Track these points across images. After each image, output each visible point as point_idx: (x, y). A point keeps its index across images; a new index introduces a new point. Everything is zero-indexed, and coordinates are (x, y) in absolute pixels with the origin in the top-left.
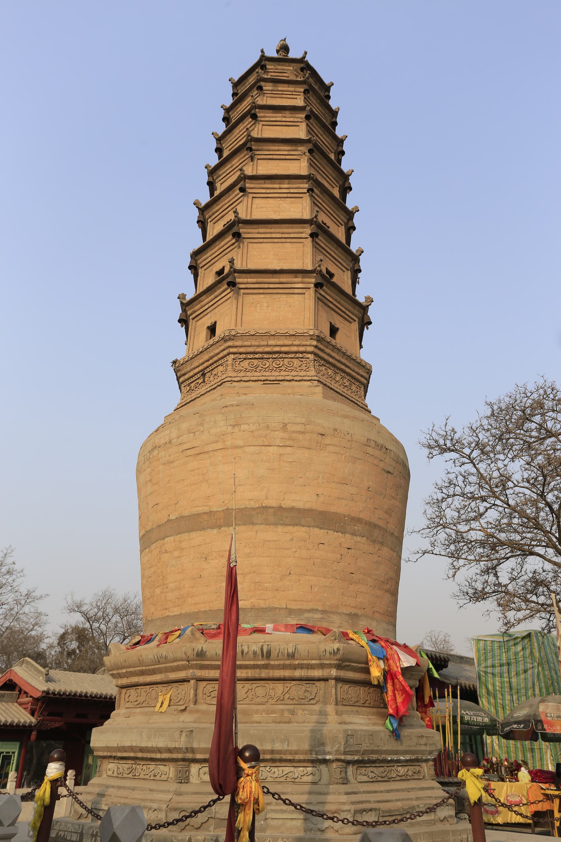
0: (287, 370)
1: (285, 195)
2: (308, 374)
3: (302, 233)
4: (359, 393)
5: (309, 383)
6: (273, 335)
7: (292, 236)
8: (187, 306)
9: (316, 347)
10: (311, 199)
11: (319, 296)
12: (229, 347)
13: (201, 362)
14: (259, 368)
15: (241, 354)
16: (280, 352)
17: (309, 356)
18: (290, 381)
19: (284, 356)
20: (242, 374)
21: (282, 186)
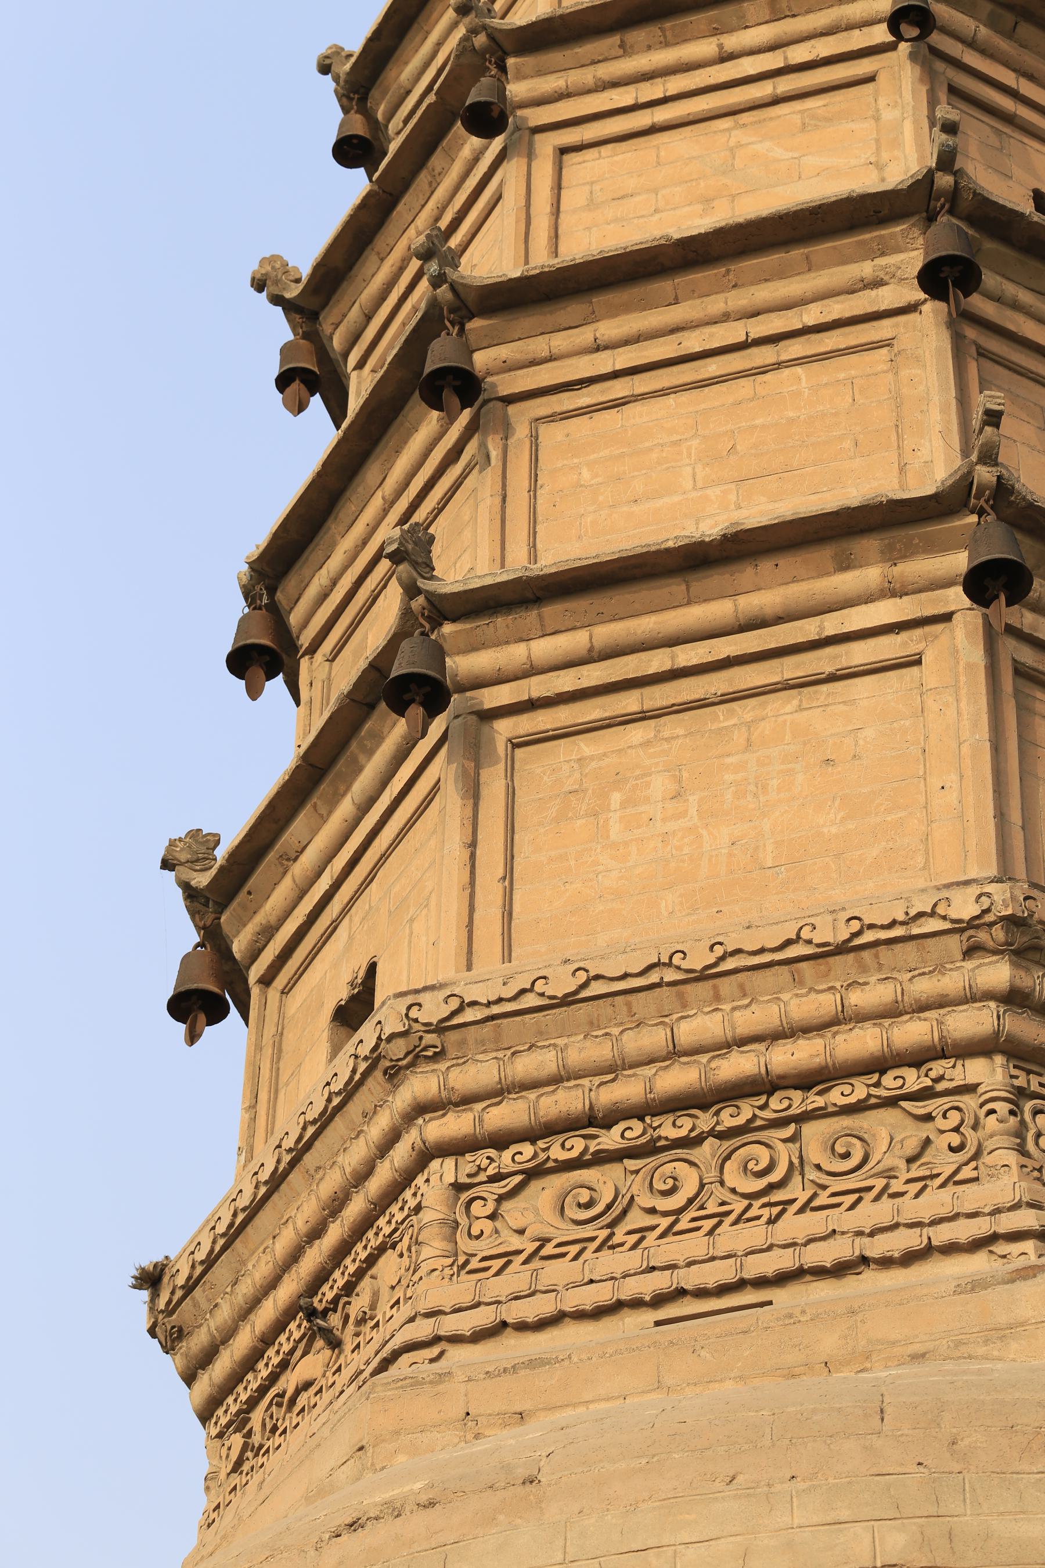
0: (823, 1199)
2: (971, 1197)
3: (877, 283)
5: (978, 1263)
6: (703, 976)
7: (812, 315)
8: (222, 907)
9: (1013, 998)
10: (930, 76)
11: (1028, 656)
12: (422, 1109)
13: (282, 1246)
14: (636, 1219)
15: (501, 1141)
17: (975, 1070)
18: (840, 1270)
19: (798, 1101)
20: (517, 1277)
21: (733, 41)
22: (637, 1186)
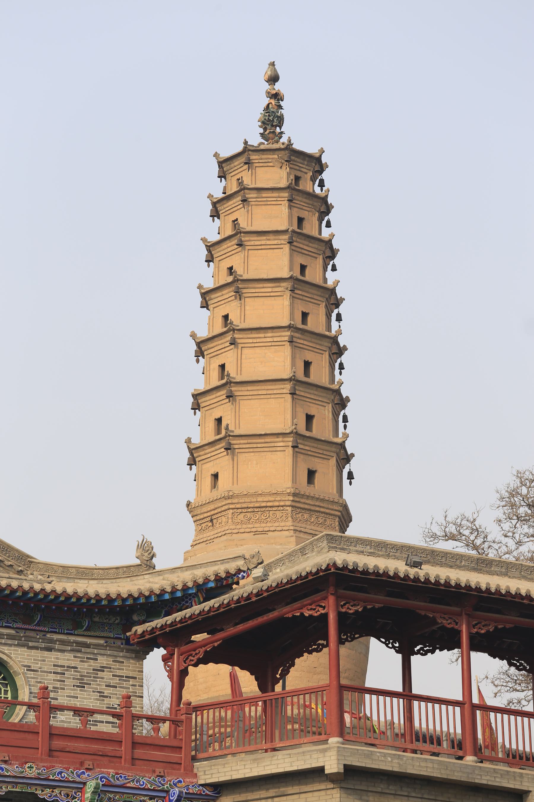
1: (270, 344)
4: (333, 525)
9: (293, 501)
13: (209, 509)
14: (252, 520)
15: (238, 509)
16: (266, 507)
17: (288, 508)
19: (270, 509)
22: (252, 516)
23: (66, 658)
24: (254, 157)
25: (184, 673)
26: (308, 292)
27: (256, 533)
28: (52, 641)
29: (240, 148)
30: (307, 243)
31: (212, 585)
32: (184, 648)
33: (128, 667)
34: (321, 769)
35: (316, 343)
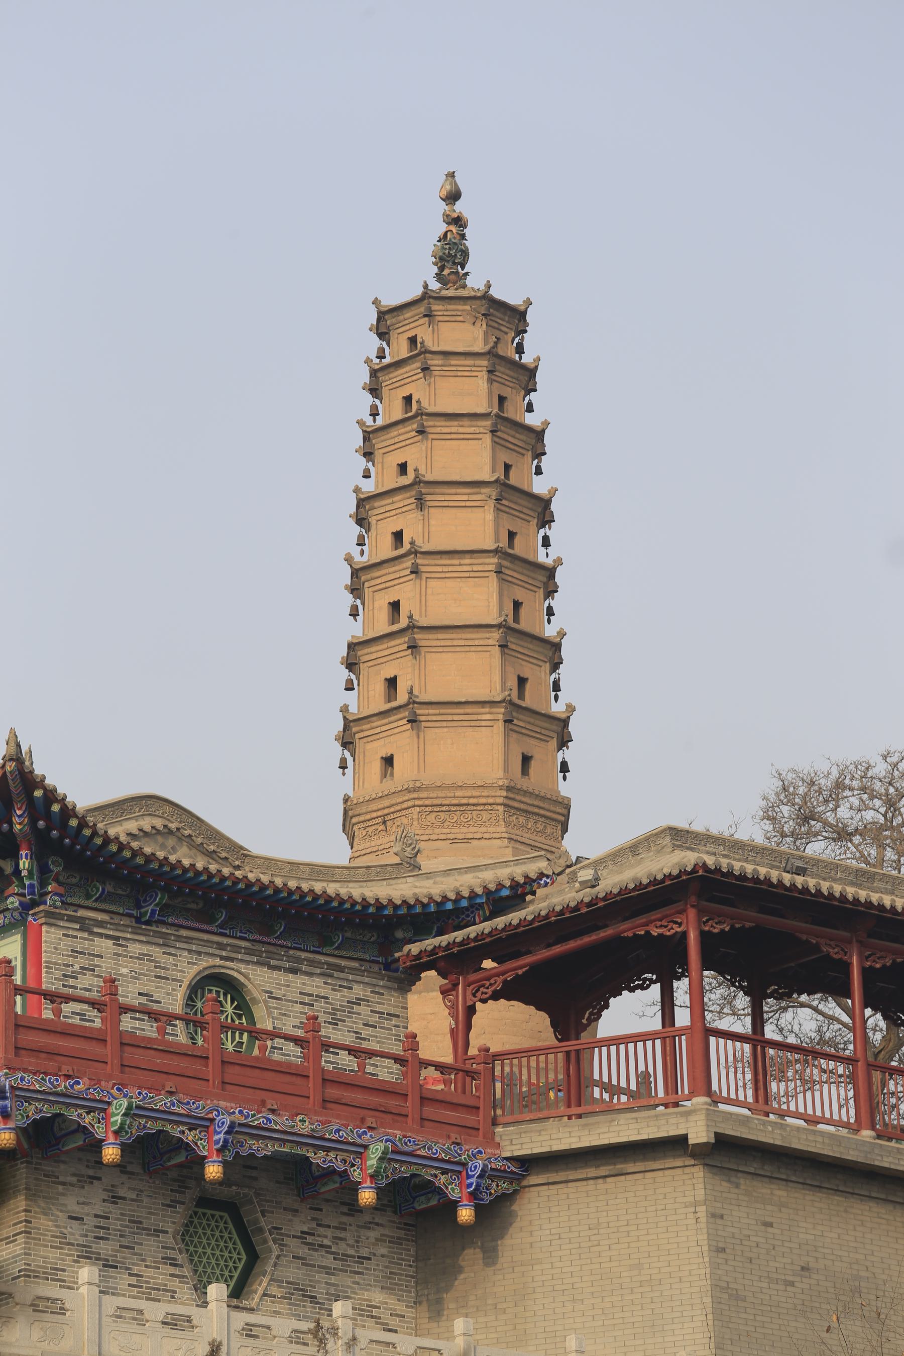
1: (467, 574)
7: (477, 643)
9: (506, 797)
15: (426, 806)
16: (468, 805)
17: (499, 807)
19: (473, 808)
23: (315, 985)
24: (437, 307)
25: (471, 1011)
26: (516, 503)
27: (454, 841)
28: (298, 960)
29: (418, 292)
30: (513, 433)
31: (505, 893)
32: (473, 977)
33: (389, 1002)
34: (684, 1138)
35: (528, 576)
